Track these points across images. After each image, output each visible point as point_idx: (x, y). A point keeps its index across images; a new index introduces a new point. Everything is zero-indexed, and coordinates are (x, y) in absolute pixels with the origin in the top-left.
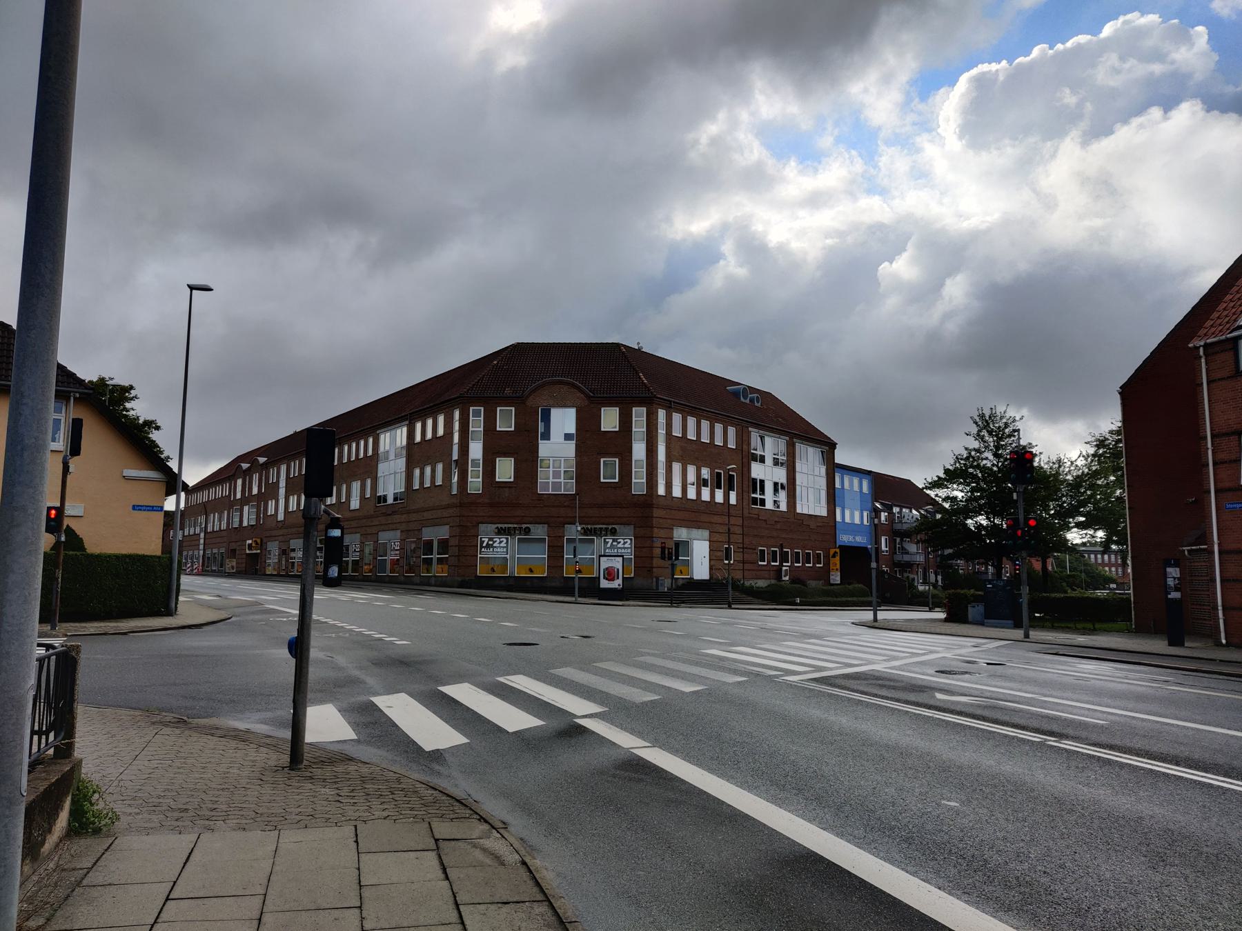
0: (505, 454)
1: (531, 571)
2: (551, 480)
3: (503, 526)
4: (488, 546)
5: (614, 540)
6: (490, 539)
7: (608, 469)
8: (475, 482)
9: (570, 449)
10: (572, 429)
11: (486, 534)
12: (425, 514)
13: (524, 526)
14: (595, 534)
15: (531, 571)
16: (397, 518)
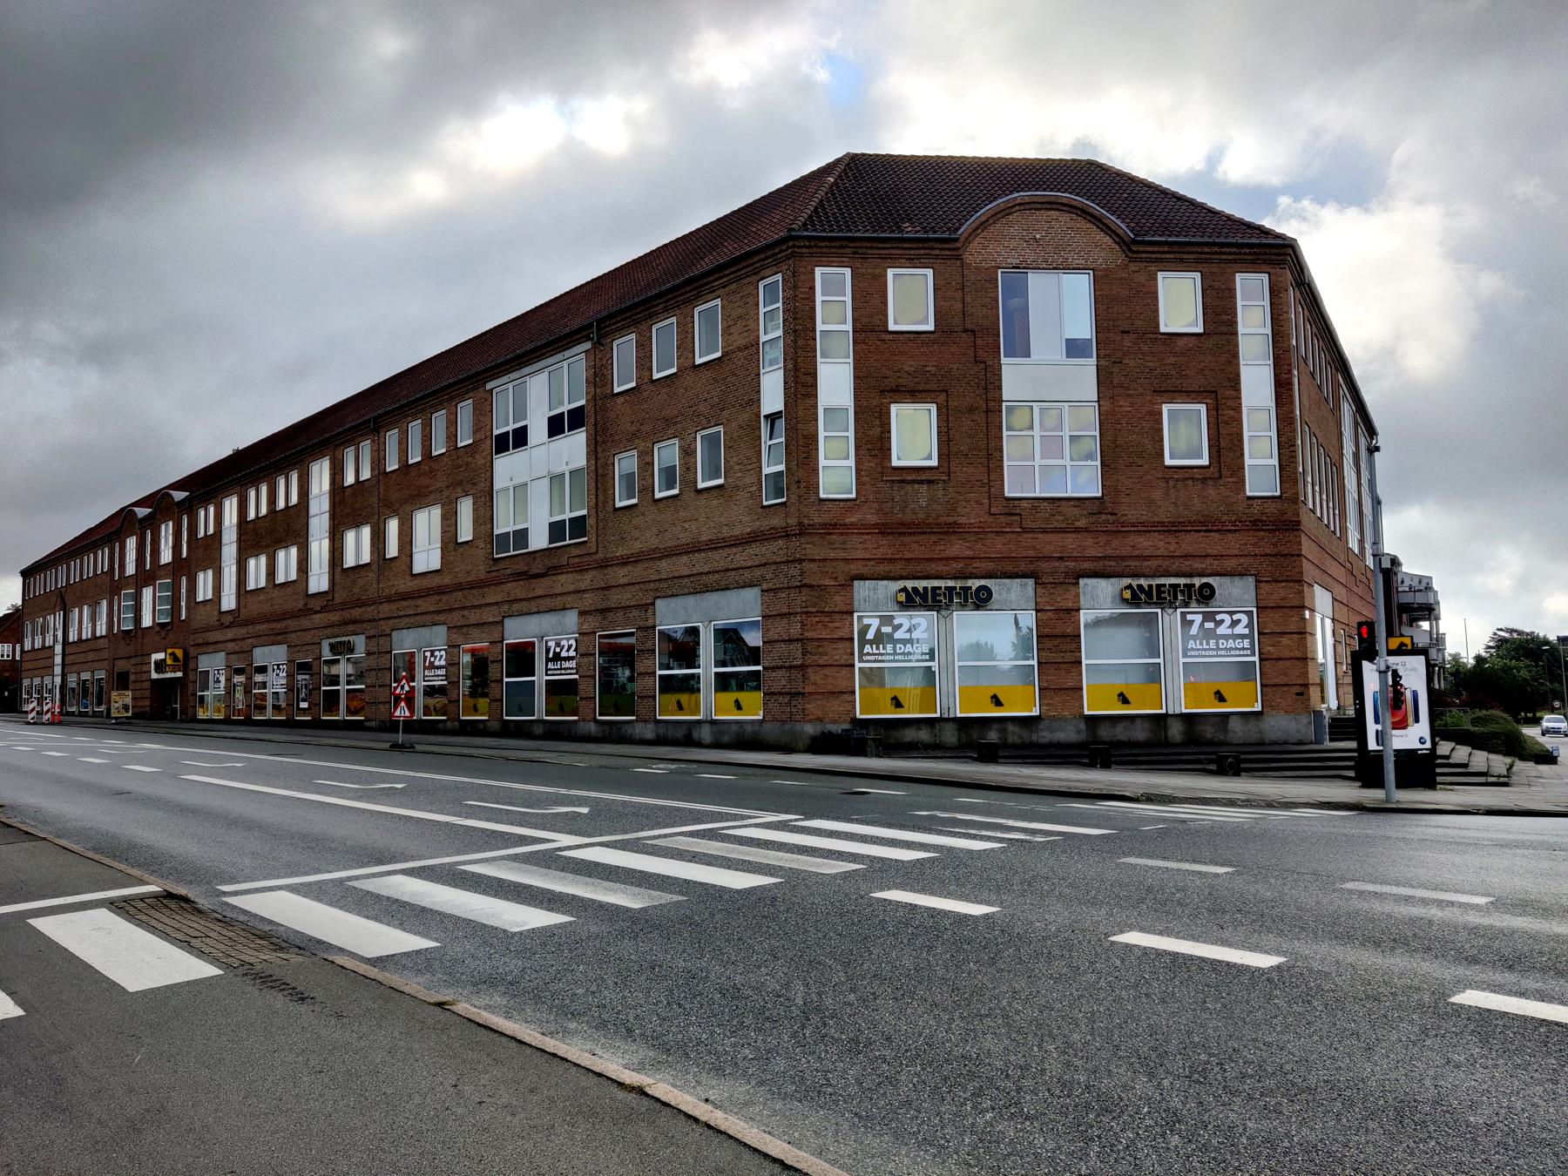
0: (913, 394)
1: (997, 702)
2: (1038, 461)
3: (921, 584)
4: (880, 639)
5: (1209, 617)
6: (886, 620)
7: (1183, 435)
8: (837, 472)
9: (1083, 379)
10: (1082, 326)
11: (872, 604)
12: (664, 564)
13: (975, 584)
14: (1161, 603)
15: (997, 702)
16: (565, 582)
